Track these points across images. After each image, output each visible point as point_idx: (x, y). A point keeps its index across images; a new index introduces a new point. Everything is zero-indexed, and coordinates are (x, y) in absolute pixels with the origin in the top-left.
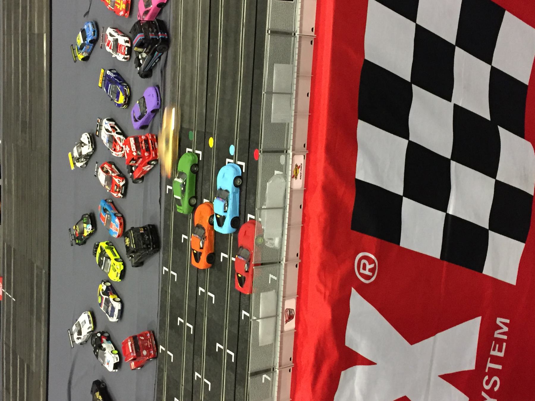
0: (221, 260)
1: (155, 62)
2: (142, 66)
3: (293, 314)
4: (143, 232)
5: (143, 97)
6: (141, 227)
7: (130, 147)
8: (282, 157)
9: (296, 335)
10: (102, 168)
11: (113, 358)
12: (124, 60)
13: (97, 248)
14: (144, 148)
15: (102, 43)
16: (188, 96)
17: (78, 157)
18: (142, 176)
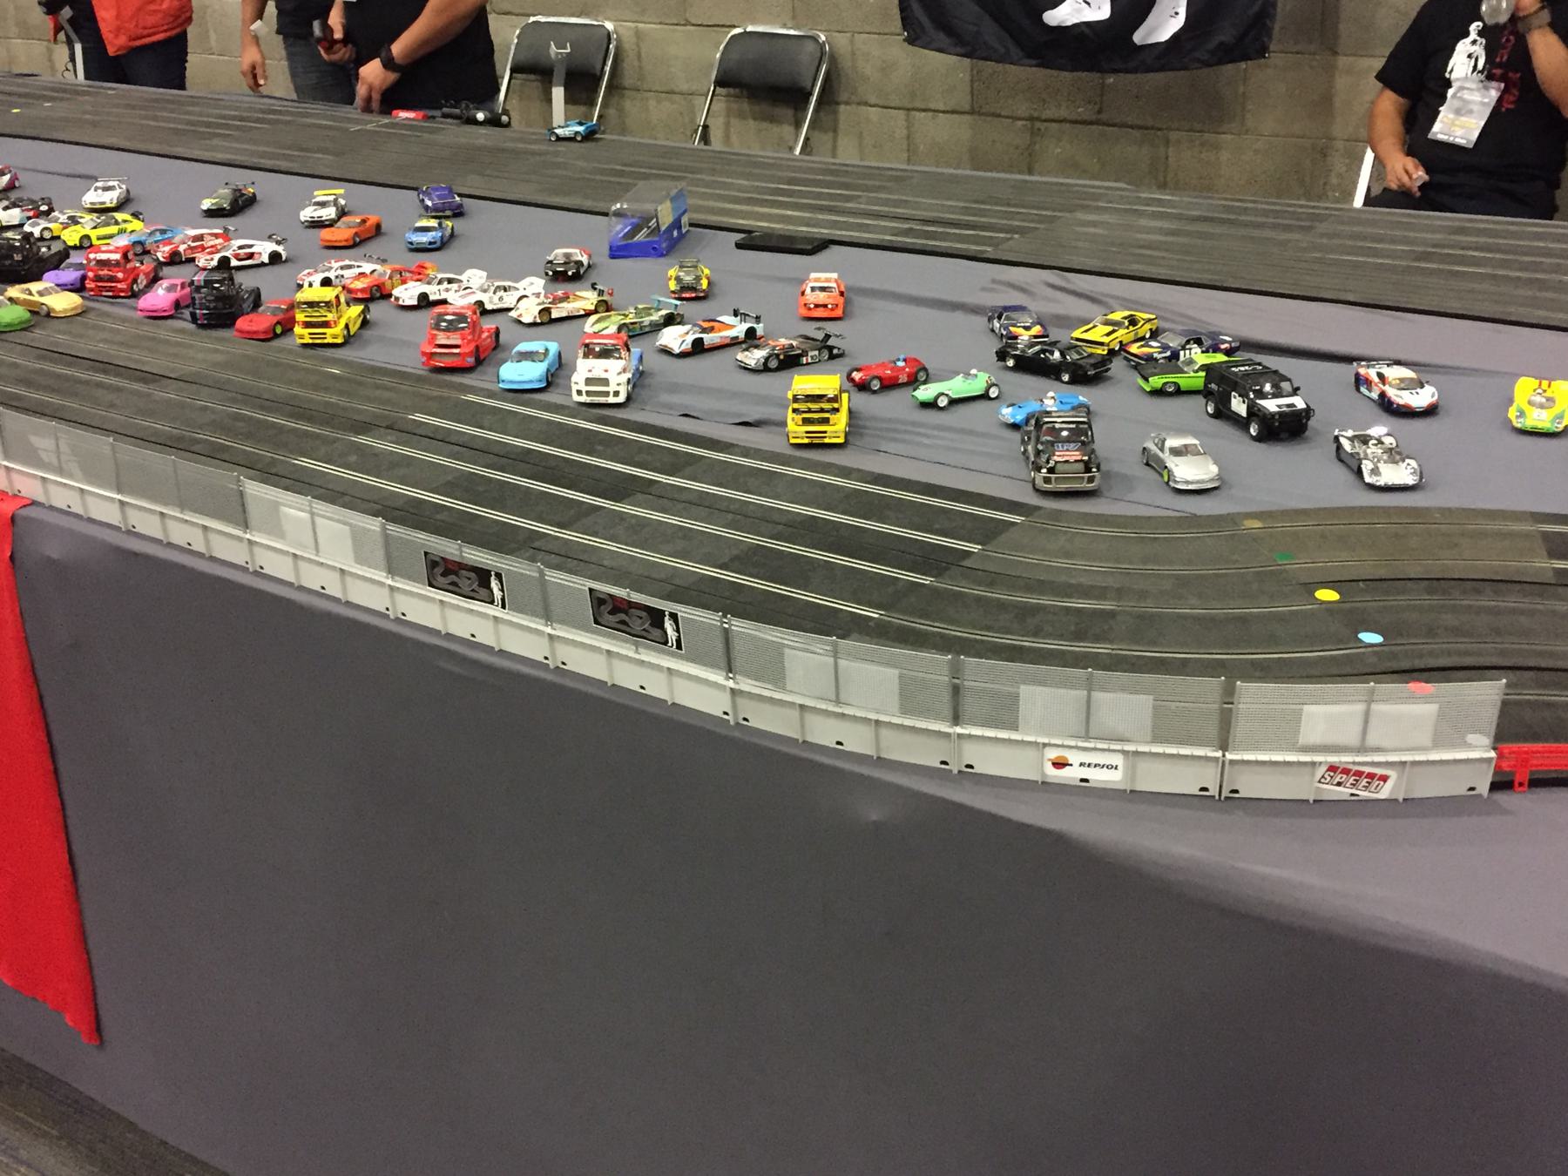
14: (101, 273)
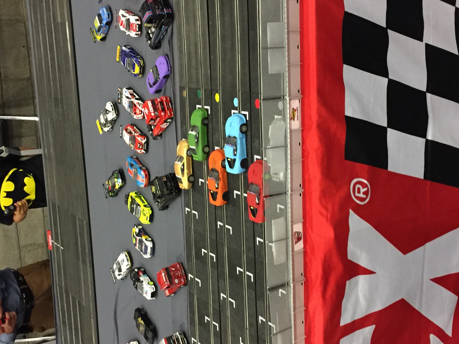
0: (235, 197)
1: (163, 34)
2: (152, 39)
3: (301, 235)
4: (166, 180)
5: (156, 66)
6: (163, 176)
7: (148, 109)
8: (280, 104)
9: (305, 253)
10: (126, 130)
11: (150, 289)
12: (136, 36)
13: (128, 198)
14: (160, 109)
15: (117, 24)
16: (194, 61)
17: (105, 123)
18: (160, 133)
